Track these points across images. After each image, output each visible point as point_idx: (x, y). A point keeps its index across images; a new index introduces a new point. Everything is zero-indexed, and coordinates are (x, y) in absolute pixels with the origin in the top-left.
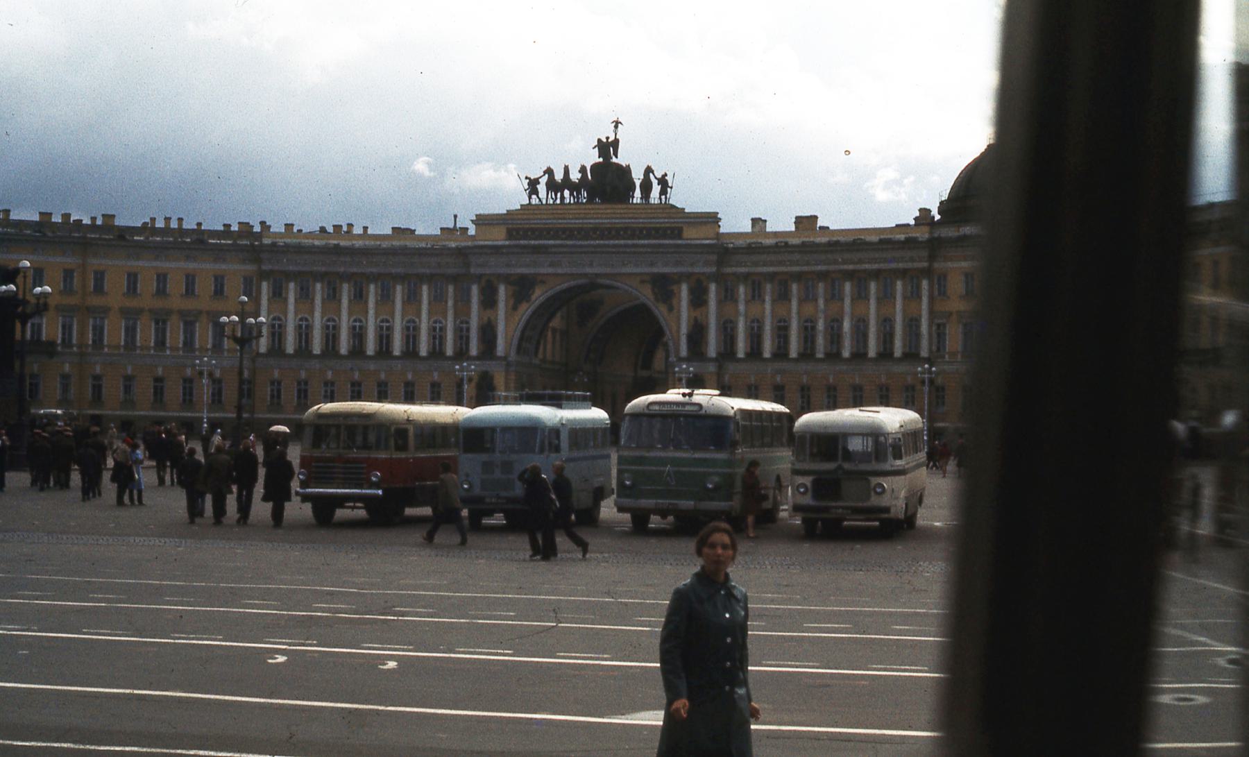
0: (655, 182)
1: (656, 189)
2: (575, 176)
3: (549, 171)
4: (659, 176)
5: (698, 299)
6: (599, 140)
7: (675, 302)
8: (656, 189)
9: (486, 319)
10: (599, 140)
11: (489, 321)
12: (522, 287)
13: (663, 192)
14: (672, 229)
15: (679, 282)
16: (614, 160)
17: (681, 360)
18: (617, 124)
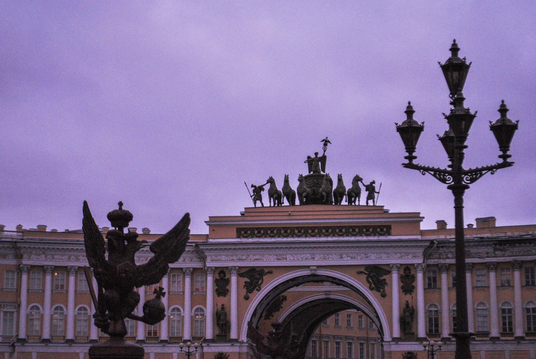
0: (363, 189)
1: (364, 194)
2: (294, 185)
3: (271, 181)
4: (367, 183)
5: (408, 287)
6: (309, 157)
7: (387, 288)
8: (364, 194)
9: (220, 306)
10: (309, 157)
11: (223, 308)
12: (253, 277)
13: (370, 197)
14: (382, 227)
15: (389, 272)
16: (322, 173)
17: (394, 339)
18: (326, 142)
